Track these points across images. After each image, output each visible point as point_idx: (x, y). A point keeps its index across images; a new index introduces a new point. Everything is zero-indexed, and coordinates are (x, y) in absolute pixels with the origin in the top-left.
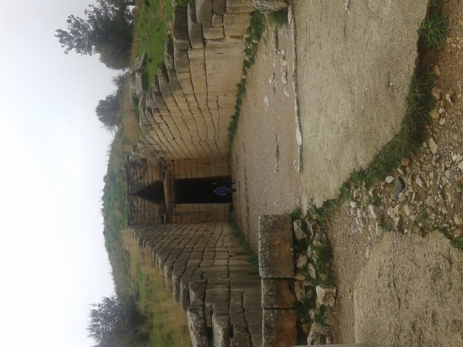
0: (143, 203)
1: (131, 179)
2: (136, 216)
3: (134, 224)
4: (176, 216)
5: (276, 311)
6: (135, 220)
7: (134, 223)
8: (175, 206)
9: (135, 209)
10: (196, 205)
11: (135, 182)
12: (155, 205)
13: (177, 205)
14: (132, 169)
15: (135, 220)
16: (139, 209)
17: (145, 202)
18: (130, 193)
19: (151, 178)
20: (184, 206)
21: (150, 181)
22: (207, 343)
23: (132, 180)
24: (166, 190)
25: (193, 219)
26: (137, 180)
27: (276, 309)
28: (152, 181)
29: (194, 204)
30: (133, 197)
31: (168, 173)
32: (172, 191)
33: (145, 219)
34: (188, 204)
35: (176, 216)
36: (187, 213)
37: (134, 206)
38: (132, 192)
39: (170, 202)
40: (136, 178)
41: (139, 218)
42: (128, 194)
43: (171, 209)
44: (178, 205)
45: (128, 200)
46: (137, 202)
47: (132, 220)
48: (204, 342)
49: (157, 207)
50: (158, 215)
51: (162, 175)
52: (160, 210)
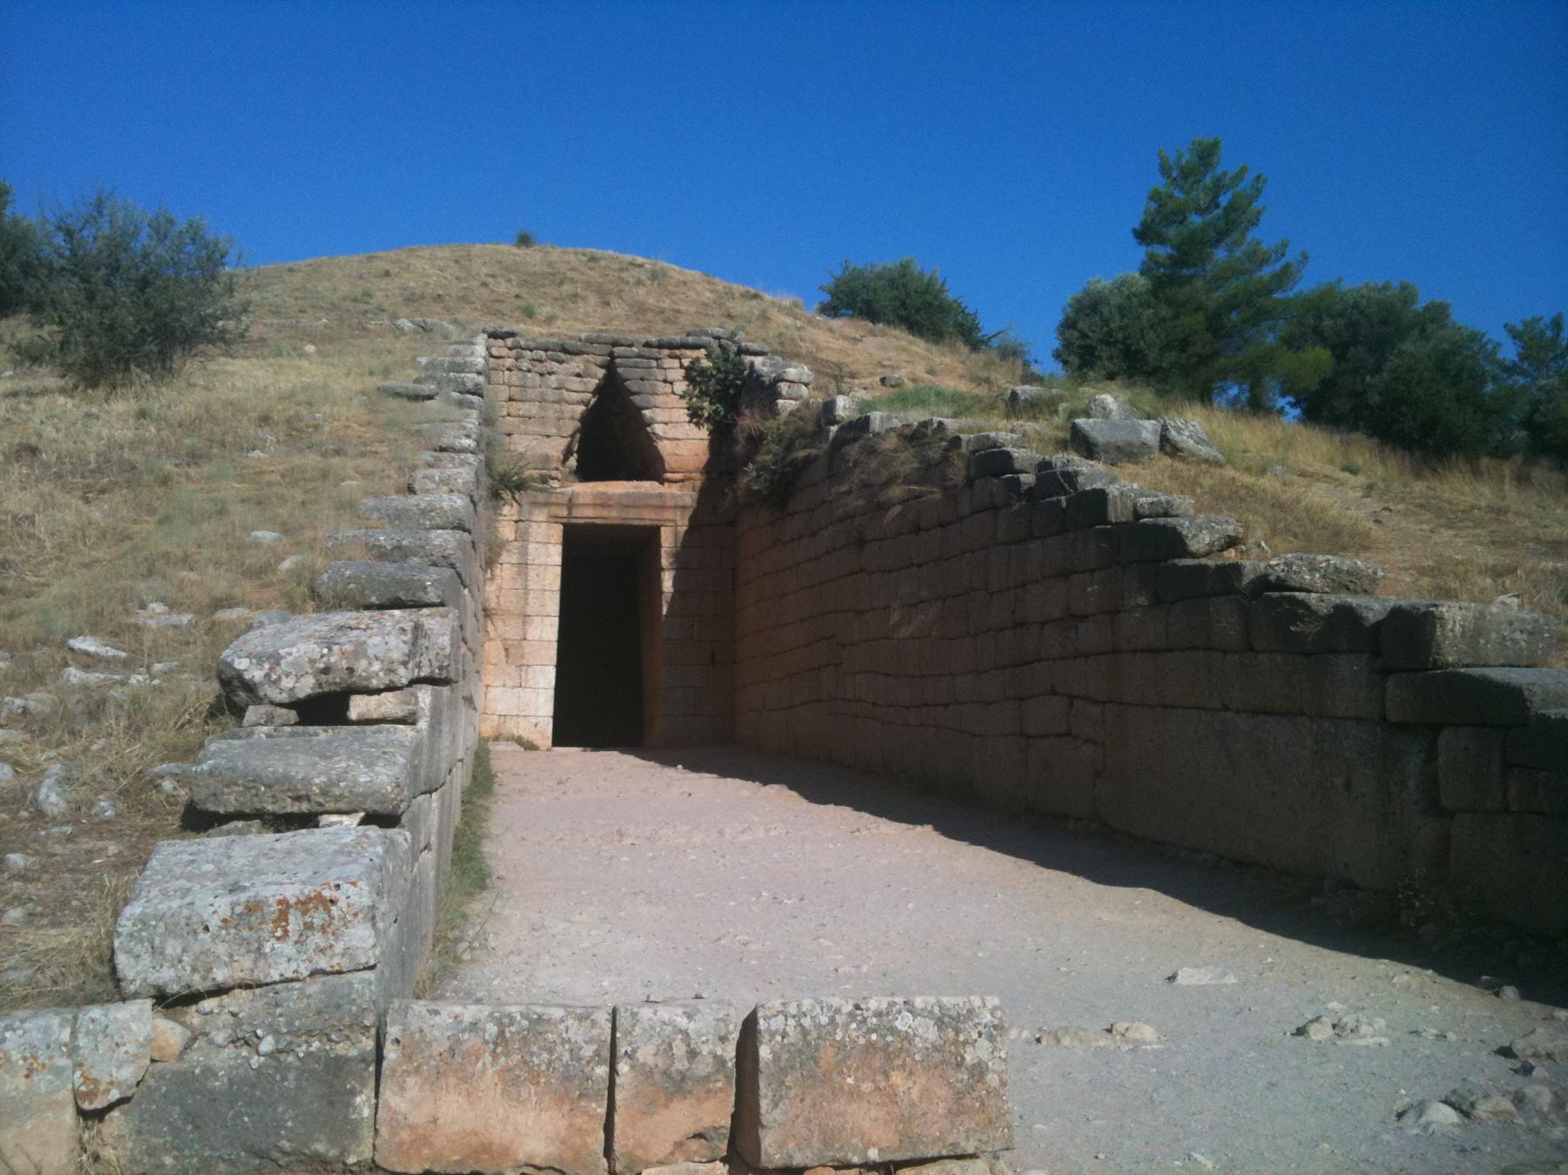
0: (575, 396)
1: (670, 357)
2: (525, 365)
5: (602, 1071)
6: (509, 362)
8: (554, 519)
10: (553, 605)
11: (660, 375)
18: (618, 350)
20: (555, 555)
21: (659, 429)
22: (284, 698)
23: (668, 363)
25: (500, 588)
26: (665, 381)
27: (613, 1071)
28: (661, 438)
29: (557, 596)
30: (599, 359)
32: (614, 514)
33: (511, 399)
34: (559, 570)
40: (671, 375)
41: (515, 377)
42: (615, 344)
43: (547, 504)
44: (557, 531)
45: (590, 341)
46: (578, 375)
48: (287, 683)
49: (556, 447)
52: (546, 459)
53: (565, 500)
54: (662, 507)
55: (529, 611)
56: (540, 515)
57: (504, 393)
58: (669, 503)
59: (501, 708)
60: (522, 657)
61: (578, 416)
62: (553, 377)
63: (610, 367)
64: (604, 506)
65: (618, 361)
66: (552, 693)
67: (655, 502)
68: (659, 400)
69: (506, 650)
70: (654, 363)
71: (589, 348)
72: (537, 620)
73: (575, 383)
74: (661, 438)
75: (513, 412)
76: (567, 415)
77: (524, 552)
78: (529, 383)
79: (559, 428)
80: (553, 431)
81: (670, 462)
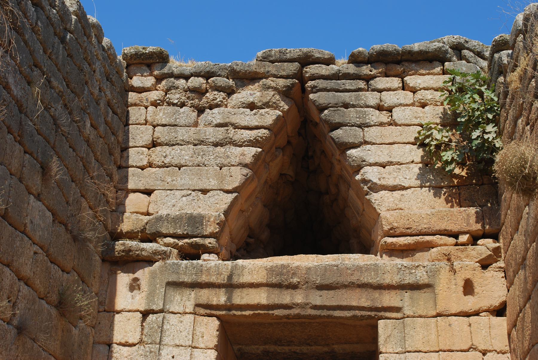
0: (247, 135)
6: (154, 95)
8: (206, 309)
9: (220, 96)
11: (372, 98)
12: (230, 197)
15: (154, 95)
16: (215, 115)
19: (391, 182)
21: (371, 174)
23: (381, 82)
26: (379, 108)
28: (376, 188)
30: (281, 83)
31: (421, 276)
32: (299, 298)
33: (154, 144)
35: (145, 314)
37: (230, 92)
38: (313, 78)
39: (230, 286)
40: (389, 98)
41: (162, 114)
46: (252, 106)
49: (214, 207)
50: (163, 212)
51: (402, 240)
53: (222, 279)
54: (380, 287)
56: (184, 301)
58: (388, 280)
61: (248, 159)
62: (216, 110)
63: (297, 93)
64: (279, 286)
65: (310, 83)
67: (366, 278)
68: (371, 133)
70: (362, 84)
71: (271, 68)
73: (248, 118)
74: (376, 188)
76: (235, 160)
78: (182, 121)
79: (222, 179)
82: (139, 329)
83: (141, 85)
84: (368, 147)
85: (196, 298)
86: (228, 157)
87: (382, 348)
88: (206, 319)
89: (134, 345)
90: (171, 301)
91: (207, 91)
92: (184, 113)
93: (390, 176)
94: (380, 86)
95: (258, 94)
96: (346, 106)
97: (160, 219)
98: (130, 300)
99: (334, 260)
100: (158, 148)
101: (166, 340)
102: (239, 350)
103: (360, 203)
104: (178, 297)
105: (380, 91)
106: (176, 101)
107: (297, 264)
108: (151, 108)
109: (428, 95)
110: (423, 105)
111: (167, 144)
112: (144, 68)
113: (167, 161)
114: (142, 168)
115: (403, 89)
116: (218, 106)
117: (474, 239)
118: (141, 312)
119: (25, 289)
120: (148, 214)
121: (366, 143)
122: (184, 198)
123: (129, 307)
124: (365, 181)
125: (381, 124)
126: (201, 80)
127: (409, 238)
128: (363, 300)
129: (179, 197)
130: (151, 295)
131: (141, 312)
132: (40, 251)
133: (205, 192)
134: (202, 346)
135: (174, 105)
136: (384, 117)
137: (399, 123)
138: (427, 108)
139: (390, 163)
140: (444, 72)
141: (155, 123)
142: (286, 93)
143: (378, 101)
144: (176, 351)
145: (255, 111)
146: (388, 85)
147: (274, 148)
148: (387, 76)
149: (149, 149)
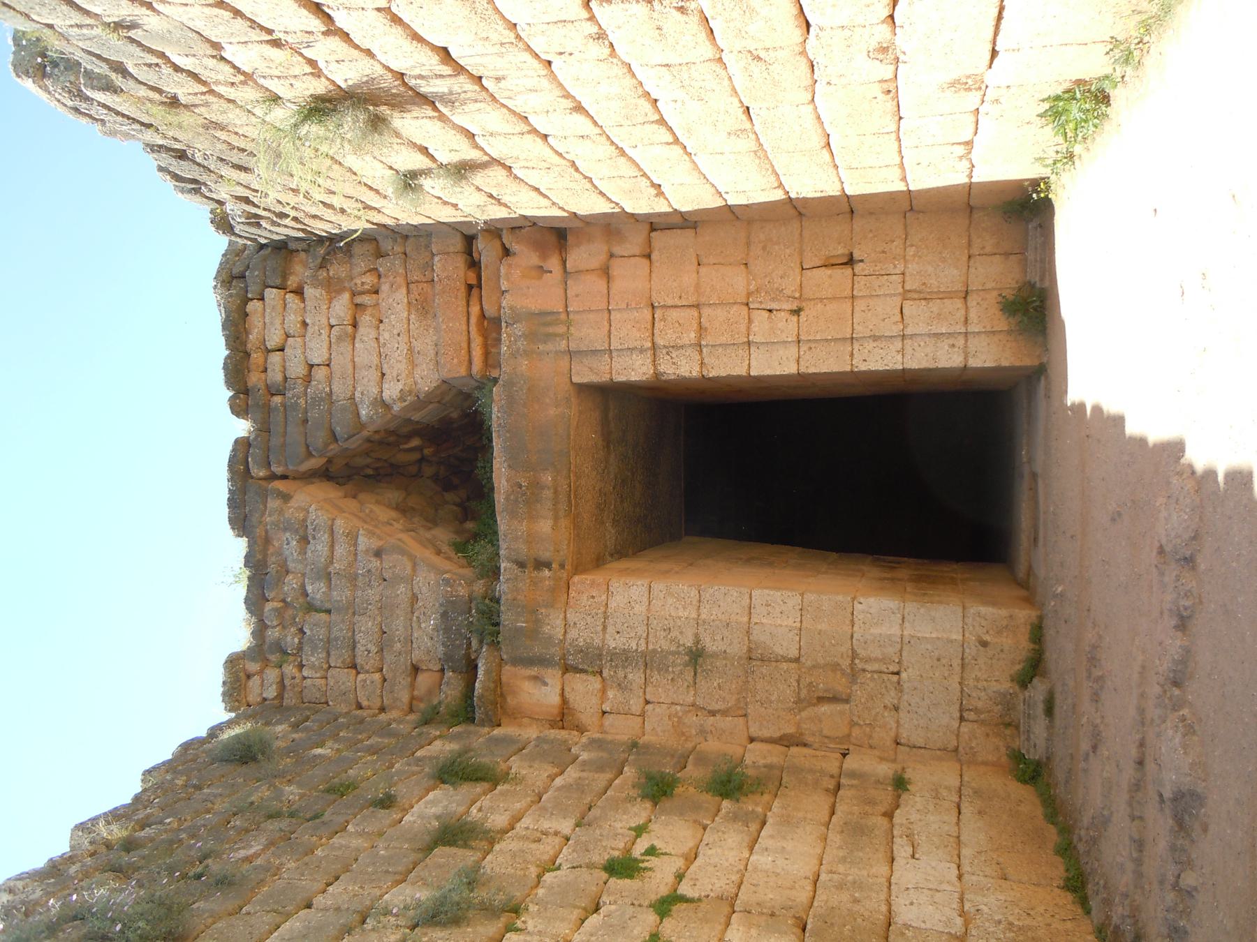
3: (280, 696)
4: (567, 669)
6: (290, 669)
7: (282, 684)
9: (291, 583)
13: (576, 579)
14: (271, 294)
16: (316, 590)
17: (353, 538)
19: (402, 367)
21: (391, 391)
24: (502, 476)
26: (308, 379)
30: (273, 504)
33: (354, 666)
34: (659, 586)
36: (649, 661)
40: (297, 369)
45: (241, 520)
46: (304, 540)
47: (266, 663)
51: (477, 353)
55: (737, 648)
57: (343, 678)
59: (946, 718)
60: (835, 667)
62: (309, 589)
66: (911, 607)
69: (821, 700)
72: (756, 631)
75: (372, 663)
76: (375, 563)
77: (624, 658)
78: (322, 633)
80: (402, 589)
81: (455, 369)
82: (583, 676)
83: (274, 687)
84: (357, 395)
85: (546, 607)
86: (369, 571)
87: (605, 378)
88: (573, 594)
89: (604, 680)
90: (550, 637)
91: (284, 601)
92: (311, 630)
93: (397, 365)
94: (279, 377)
95: (288, 535)
96: (306, 421)
97: (448, 658)
98: (548, 688)
99: (499, 437)
100: (359, 661)
101: (597, 642)
102: (612, 555)
103: (431, 406)
104: (546, 629)
105: (285, 378)
106: (296, 640)
107: (504, 482)
108: (305, 673)
109: (293, 320)
110: (305, 324)
111: (354, 648)
112: (251, 683)
113: (374, 649)
114: (385, 680)
115: (282, 350)
116: (303, 586)
117: (474, 264)
118: (564, 674)
119: (526, 821)
120: (442, 670)
121: (352, 398)
122: (423, 625)
123: (558, 690)
124: (402, 399)
125: (330, 379)
126: (269, 606)
127: (472, 345)
128: (548, 400)
129: (420, 633)
130: (543, 662)
131: (564, 674)
132: (478, 804)
133: (414, 598)
134: (604, 597)
135: (300, 643)
136: (320, 374)
137: (327, 356)
138: (308, 321)
139: (380, 367)
140: (262, 299)
141: (325, 666)
142: (286, 498)
143: (300, 381)
144: (610, 629)
145: (310, 538)
146: (278, 368)
147: (361, 515)
148: (265, 370)
149: (358, 673)
